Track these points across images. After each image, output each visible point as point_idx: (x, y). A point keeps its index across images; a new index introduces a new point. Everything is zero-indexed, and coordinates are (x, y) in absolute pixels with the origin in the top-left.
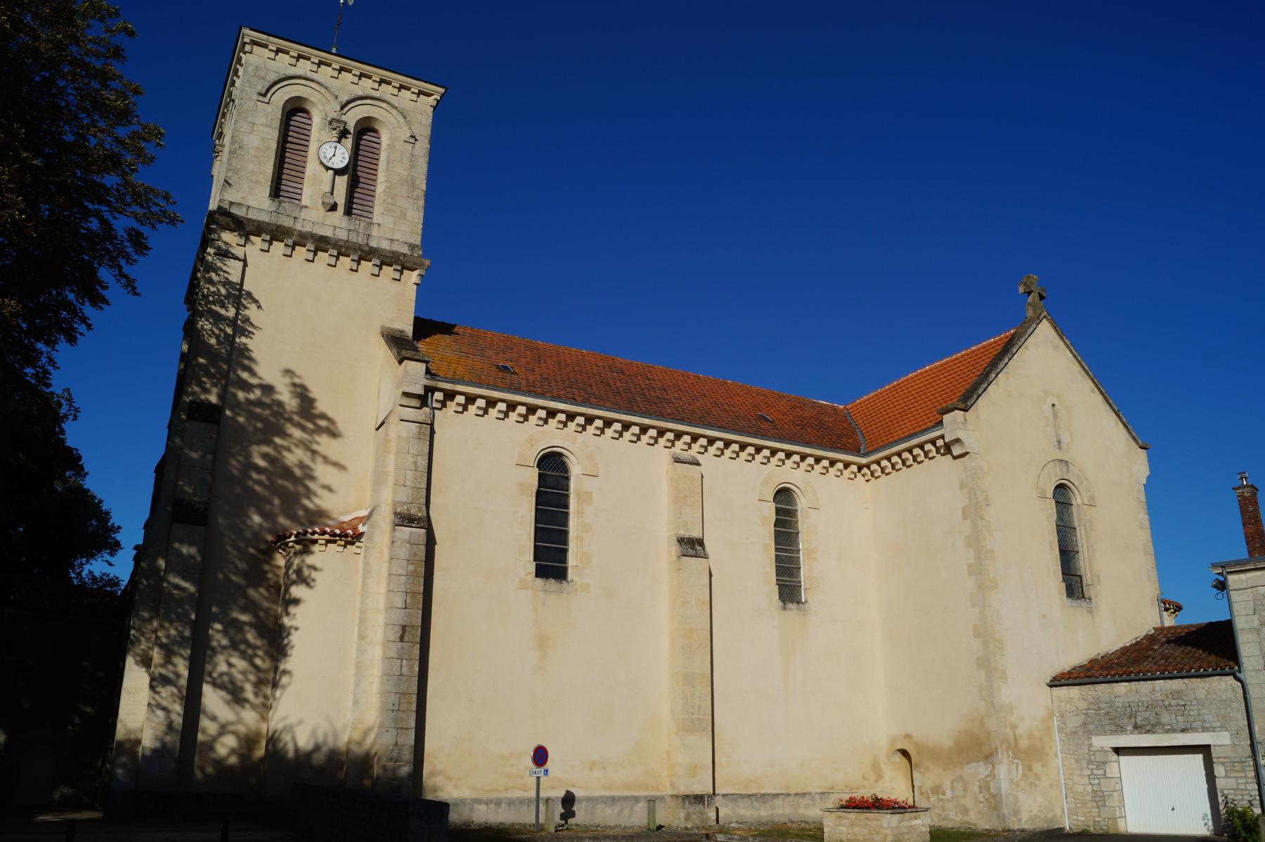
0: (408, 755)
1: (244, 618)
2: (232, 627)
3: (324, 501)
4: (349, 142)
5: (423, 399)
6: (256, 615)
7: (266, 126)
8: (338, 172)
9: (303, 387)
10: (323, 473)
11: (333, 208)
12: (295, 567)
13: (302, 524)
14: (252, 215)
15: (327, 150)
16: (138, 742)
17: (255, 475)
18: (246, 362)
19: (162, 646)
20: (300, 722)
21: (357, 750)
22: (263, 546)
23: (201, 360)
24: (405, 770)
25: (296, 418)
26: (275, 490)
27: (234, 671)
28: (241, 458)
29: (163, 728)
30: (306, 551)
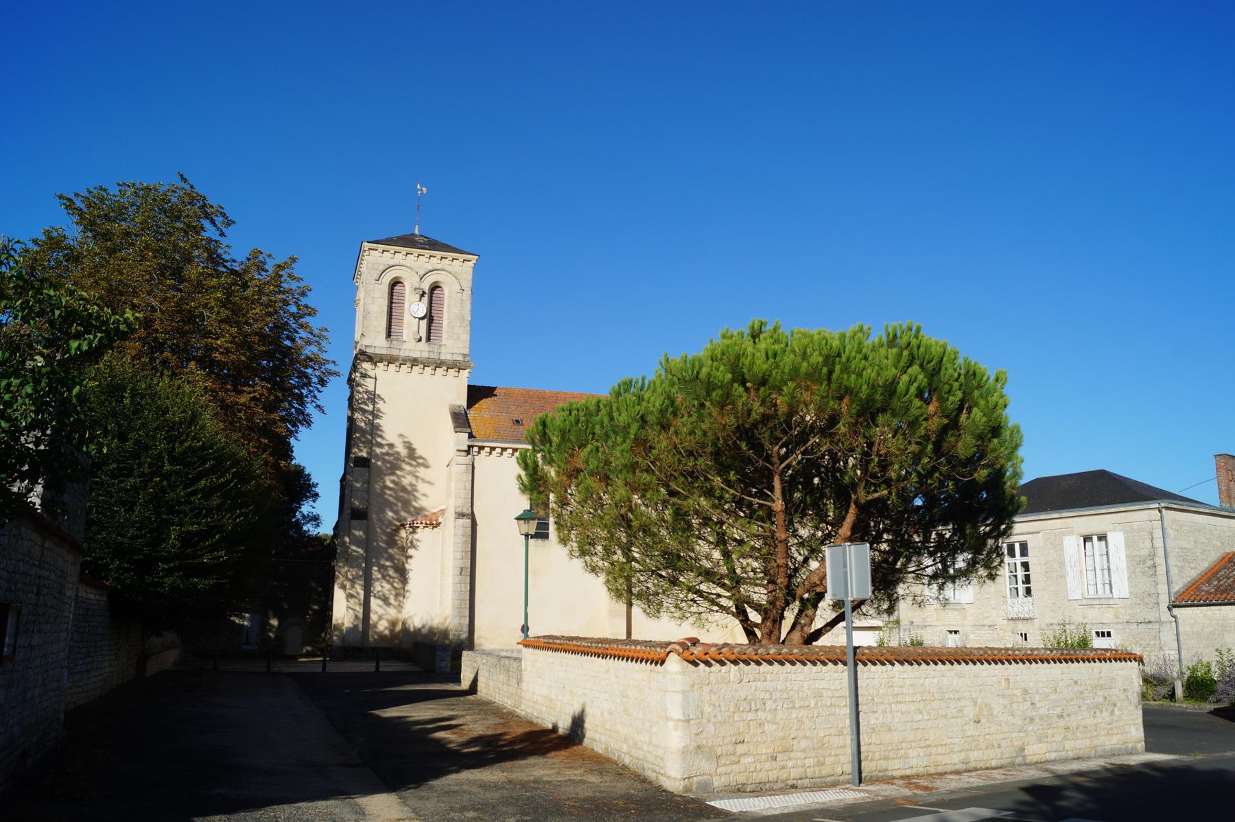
0: (466, 629)
1: (388, 563)
2: (382, 568)
3: (422, 502)
4: (426, 299)
5: (468, 452)
6: (393, 562)
7: (380, 298)
8: (420, 319)
9: (409, 443)
10: (422, 487)
11: (420, 340)
12: (410, 540)
13: (412, 515)
14: (378, 351)
15: (414, 307)
16: (343, 624)
17: (388, 492)
18: (379, 433)
19: (350, 580)
20: (415, 614)
21: (442, 627)
22: (394, 528)
23: (358, 435)
24: (464, 636)
25: (407, 460)
26: (398, 498)
27: (384, 589)
28: (381, 484)
29: (353, 617)
30: (414, 532)
